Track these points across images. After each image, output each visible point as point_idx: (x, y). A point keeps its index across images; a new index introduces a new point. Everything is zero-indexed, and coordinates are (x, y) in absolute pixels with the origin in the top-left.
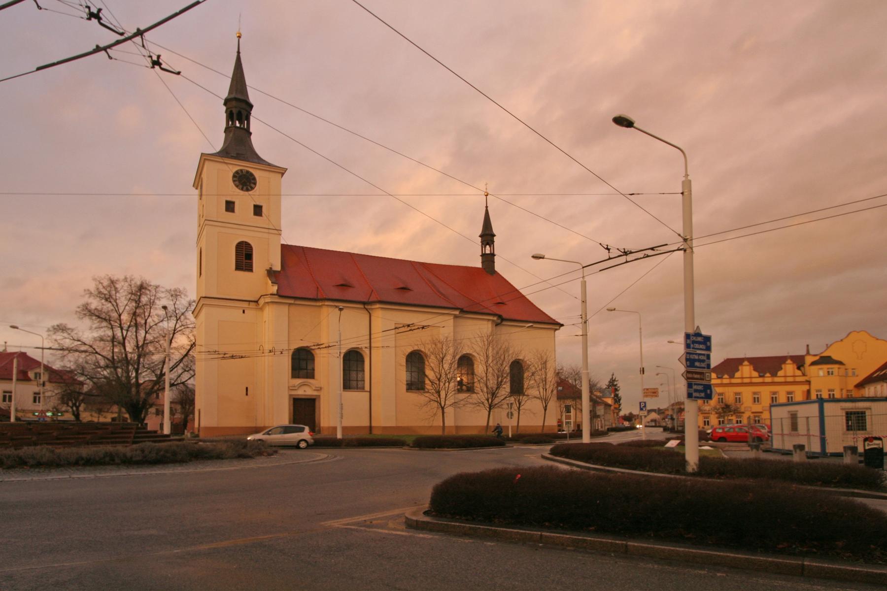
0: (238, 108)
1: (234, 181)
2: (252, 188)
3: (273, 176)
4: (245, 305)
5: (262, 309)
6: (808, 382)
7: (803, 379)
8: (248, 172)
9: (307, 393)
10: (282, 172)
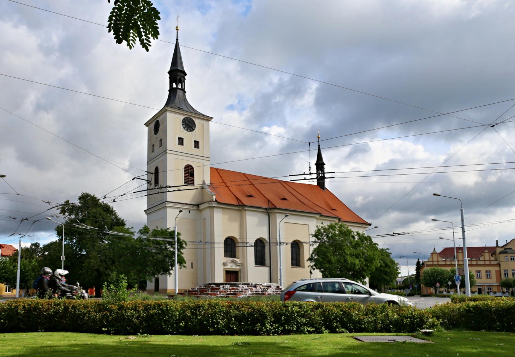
0: (177, 75)
1: (183, 125)
2: (193, 130)
3: (205, 122)
4: (190, 207)
5: (200, 211)
6: (499, 265)
7: (495, 263)
8: (191, 119)
9: (232, 267)
10: (209, 119)
